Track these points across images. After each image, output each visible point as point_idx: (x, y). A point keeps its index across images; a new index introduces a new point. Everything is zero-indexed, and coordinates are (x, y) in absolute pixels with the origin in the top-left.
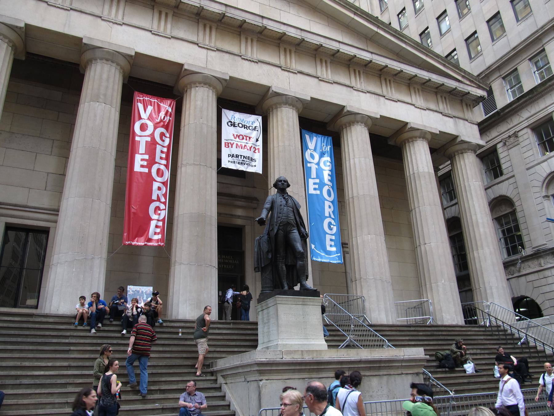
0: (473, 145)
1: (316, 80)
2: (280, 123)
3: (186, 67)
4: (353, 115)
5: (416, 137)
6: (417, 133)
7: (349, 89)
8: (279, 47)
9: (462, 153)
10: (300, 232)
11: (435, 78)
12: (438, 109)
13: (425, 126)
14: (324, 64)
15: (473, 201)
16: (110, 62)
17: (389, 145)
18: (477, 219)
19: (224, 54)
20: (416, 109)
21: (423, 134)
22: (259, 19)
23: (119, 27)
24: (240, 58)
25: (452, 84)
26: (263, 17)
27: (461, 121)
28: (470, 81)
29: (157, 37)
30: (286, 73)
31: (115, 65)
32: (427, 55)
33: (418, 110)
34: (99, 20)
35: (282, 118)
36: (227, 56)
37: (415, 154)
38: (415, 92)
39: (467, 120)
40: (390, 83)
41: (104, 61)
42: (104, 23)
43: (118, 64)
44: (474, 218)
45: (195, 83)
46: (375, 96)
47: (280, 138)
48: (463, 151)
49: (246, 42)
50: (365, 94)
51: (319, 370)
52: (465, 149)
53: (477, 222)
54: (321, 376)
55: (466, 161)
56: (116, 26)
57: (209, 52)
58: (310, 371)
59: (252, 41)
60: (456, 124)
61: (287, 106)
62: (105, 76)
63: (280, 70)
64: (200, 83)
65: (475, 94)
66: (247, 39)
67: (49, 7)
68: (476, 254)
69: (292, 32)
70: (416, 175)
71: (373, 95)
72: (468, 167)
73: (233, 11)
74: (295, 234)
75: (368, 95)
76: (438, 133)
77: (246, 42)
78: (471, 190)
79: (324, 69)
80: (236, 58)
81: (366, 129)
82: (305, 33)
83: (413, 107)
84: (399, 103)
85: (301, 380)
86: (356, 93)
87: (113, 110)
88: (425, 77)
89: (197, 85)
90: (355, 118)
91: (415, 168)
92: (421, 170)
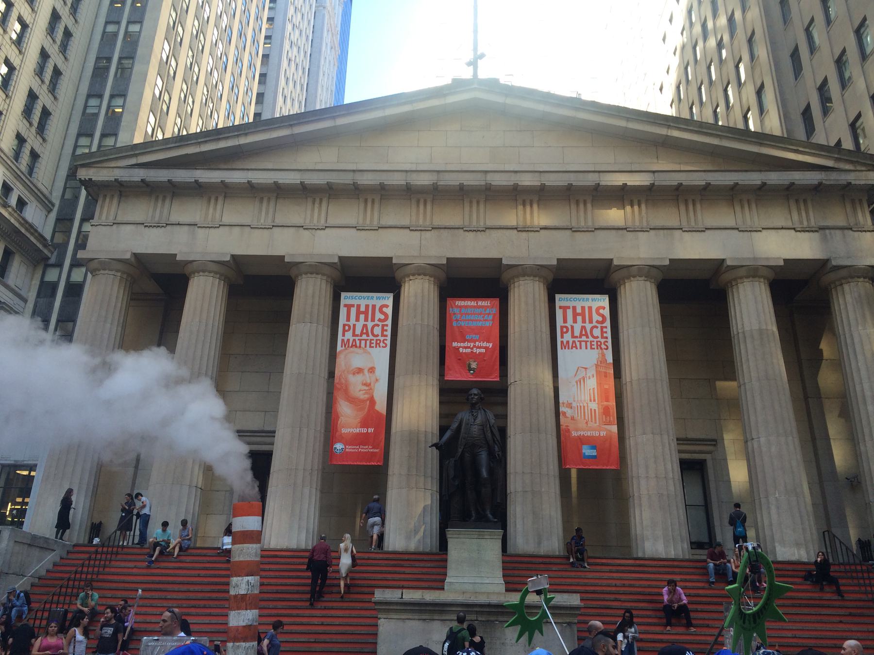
0: (860, 269)
1: (568, 232)
2: (516, 301)
3: (394, 261)
4: (625, 270)
5: (741, 278)
6: (742, 272)
7: (620, 232)
8: (516, 200)
9: (841, 285)
10: (491, 454)
11: (774, 178)
12: (790, 224)
13: (755, 259)
14: (581, 206)
15: (857, 362)
16: (314, 275)
17: (694, 298)
18: (863, 390)
19: (442, 231)
20: (742, 233)
21: (753, 272)
22: (479, 176)
23: (322, 231)
24: (461, 231)
25: (812, 178)
26: (486, 172)
27: (838, 232)
28: (852, 162)
29: (363, 232)
30: (524, 234)
31: (320, 276)
32: (761, 144)
33: (746, 233)
34: (301, 229)
35: (519, 296)
36: (445, 233)
37: (740, 303)
38: (742, 207)
39: (851, 229)
40: (694, 205)
41: (309, 275)
42: (306, 232)
43: (323, 275)
44: (858, 388)
45: (408, 276)
46: (665, 231)
47: (516, 321)
48: (843, 281)
49: (471, 207)
50: (646, 233)
51: (442, 612)
52: (843, 278)
53: (864, 396)
54: (444, 618)
55: (848, 298)
56: (318, 231)
57: (423, 233)
58: (431, 612)
59: (478, 203)
60: (824, 239)
61: (526, 278)
62: (310, 292)
63: (515, 231)
64: (413, 275)
65: (862, 183)
66: (471, 202)
67: (253, 230)
68: (862, 448)
69: (527, 181)
70: (741, 335)
71: (662, 231)
72: (850, 307)
73: (447, 176)
74: (483, 456)
75: (652, 232)
76: (782, 263)
77: (471, 207)
78: (853, 344)
79: (582, 213)
80: (456, 231)
81: (648, 283)
82: (547, 175)
83: (736, 231)
84: (708, 232)
85: (421, 622)
86: (630, 235)
87: (320, 327)
88: (754, 182)
89: (411, 277)
90: (629, 271)
91: (739, 327)
92: (747, 328)
